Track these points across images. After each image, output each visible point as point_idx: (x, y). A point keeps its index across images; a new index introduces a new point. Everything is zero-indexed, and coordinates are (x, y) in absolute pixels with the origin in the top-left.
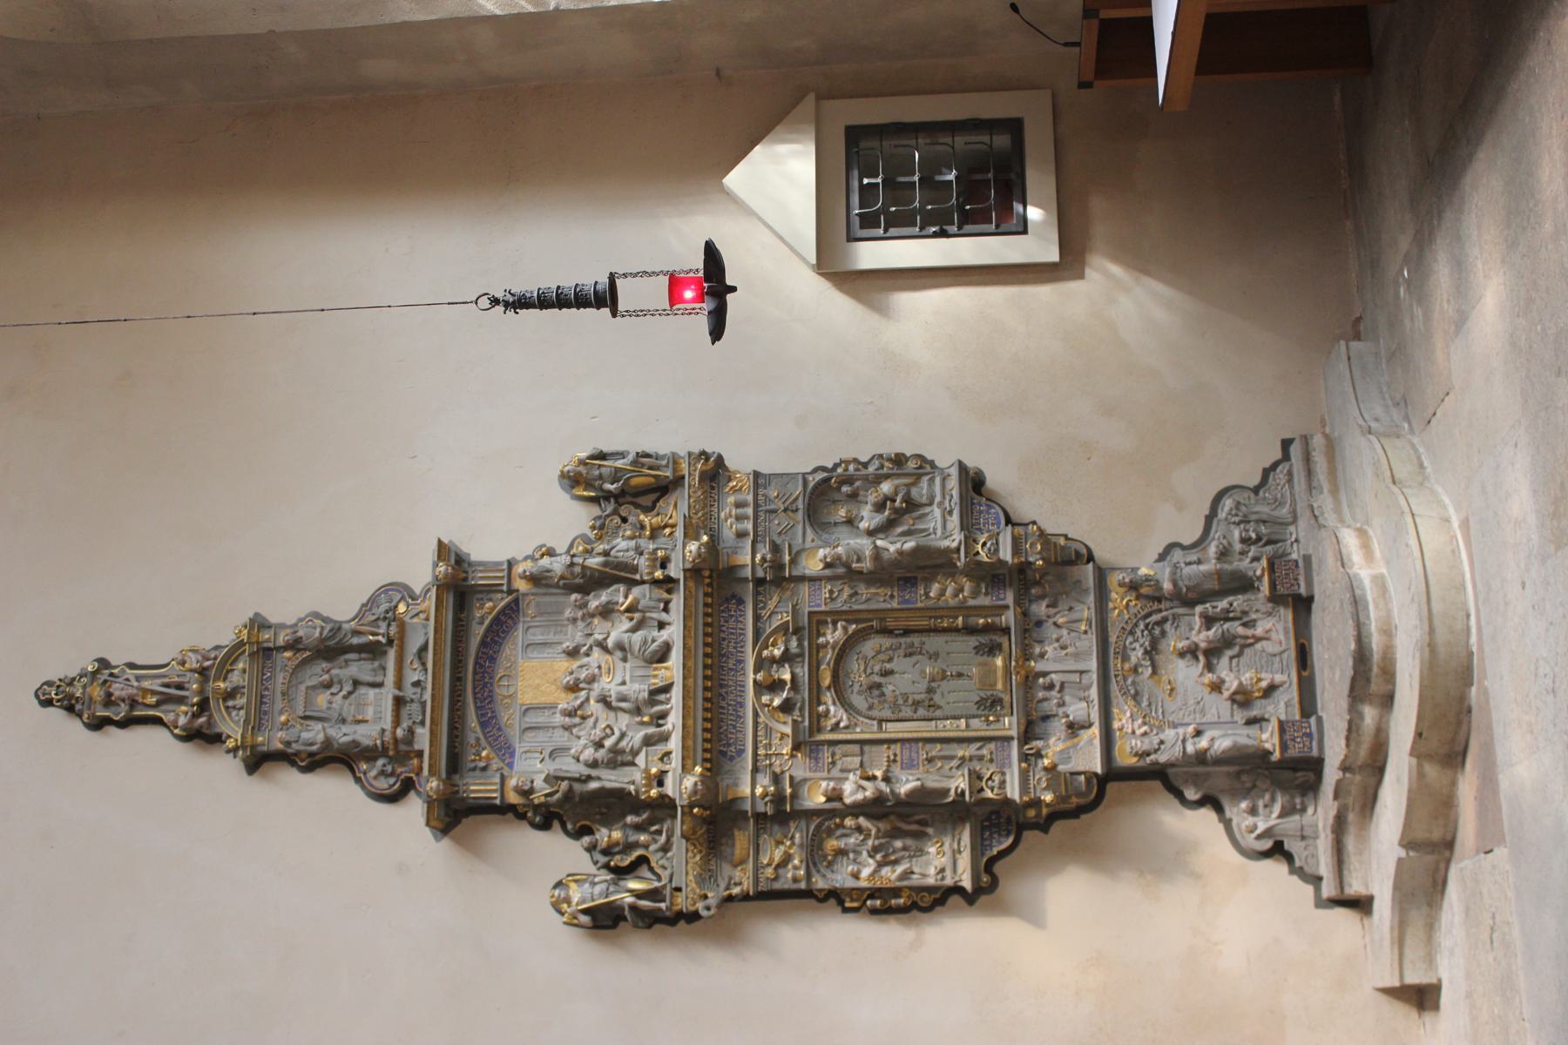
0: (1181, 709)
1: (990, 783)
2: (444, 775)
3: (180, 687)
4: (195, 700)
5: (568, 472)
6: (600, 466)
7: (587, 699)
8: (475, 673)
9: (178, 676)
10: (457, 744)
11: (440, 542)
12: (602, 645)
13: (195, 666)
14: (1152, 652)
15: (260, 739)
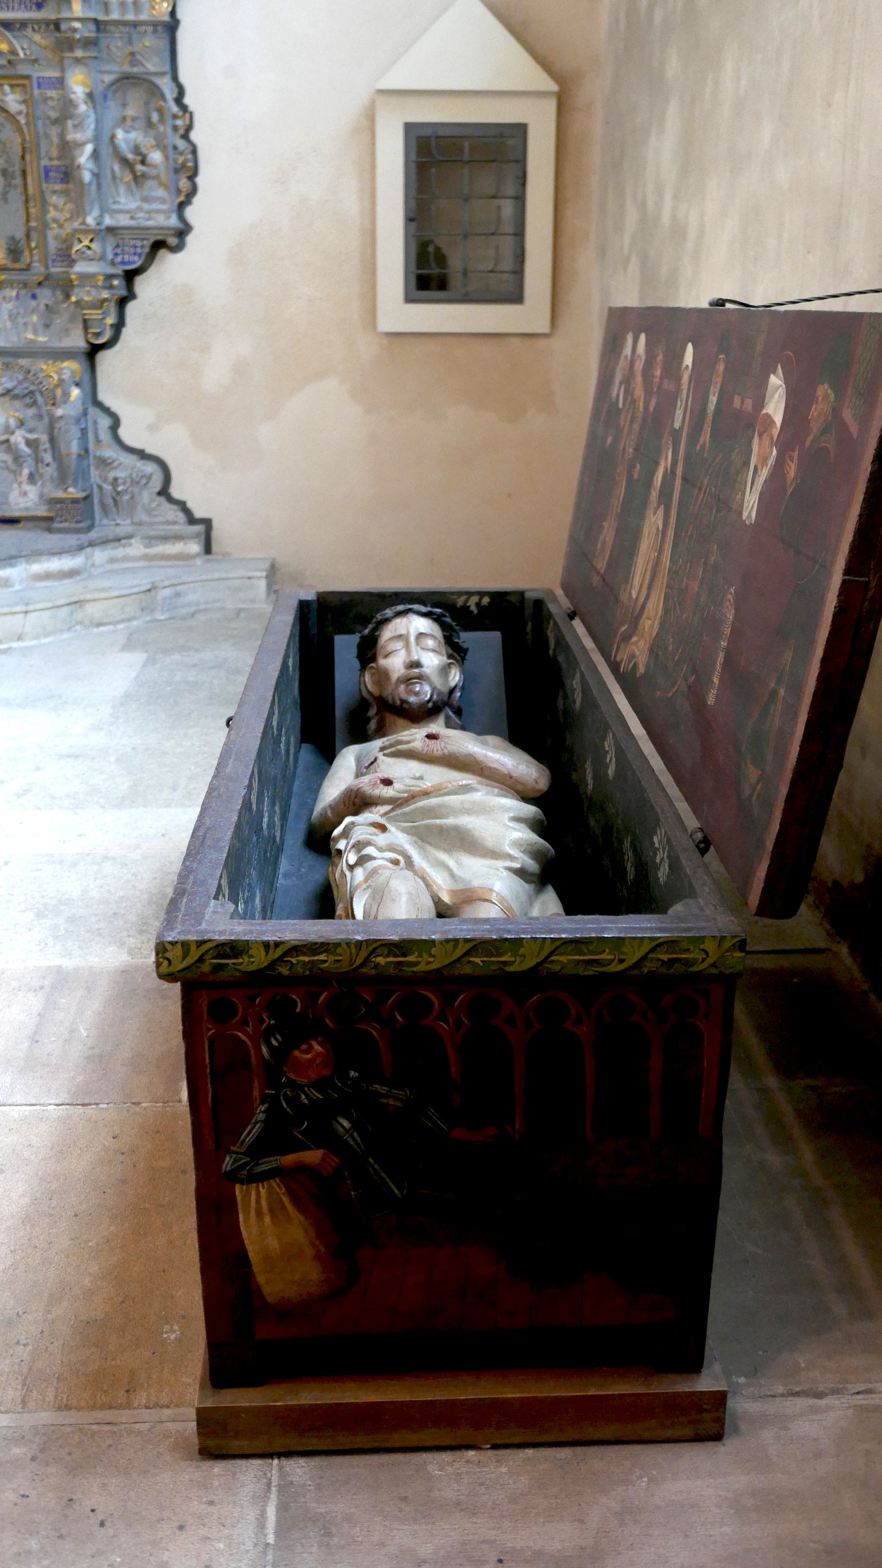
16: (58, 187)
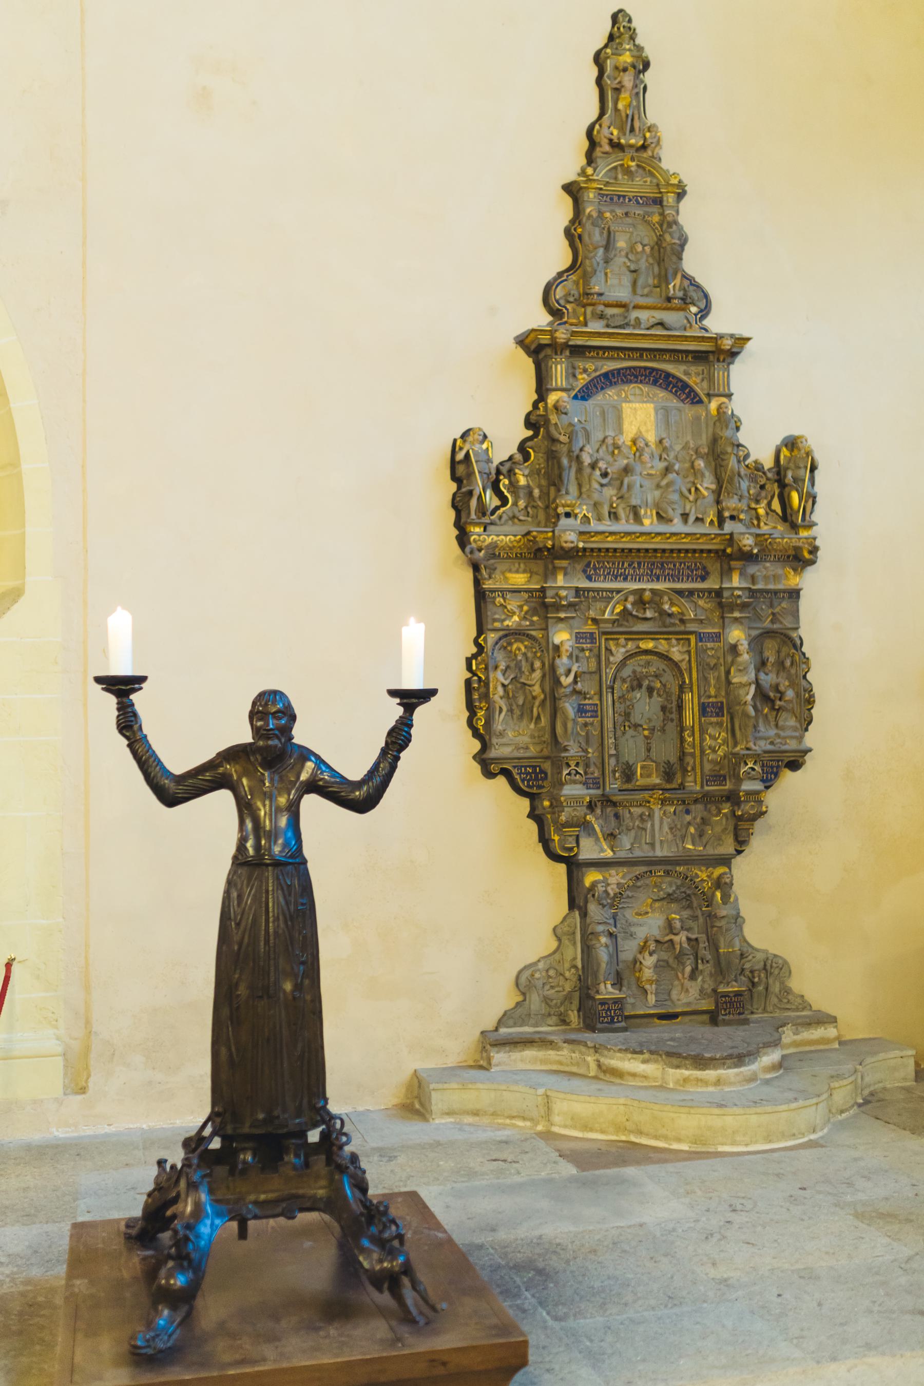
0: (627, 921)
1: (574, 772)
2: (571, 343)
3: (632, 130)
4: (623, 141)
5: (802, 442)
6: (806, 467)
8: (645, 368)
9: (640, 128)
10: (592, 354)
11: (749, 339)
12: (668, 470)
13: (649, 141)
15: (591, 195)
16: (714, 719)
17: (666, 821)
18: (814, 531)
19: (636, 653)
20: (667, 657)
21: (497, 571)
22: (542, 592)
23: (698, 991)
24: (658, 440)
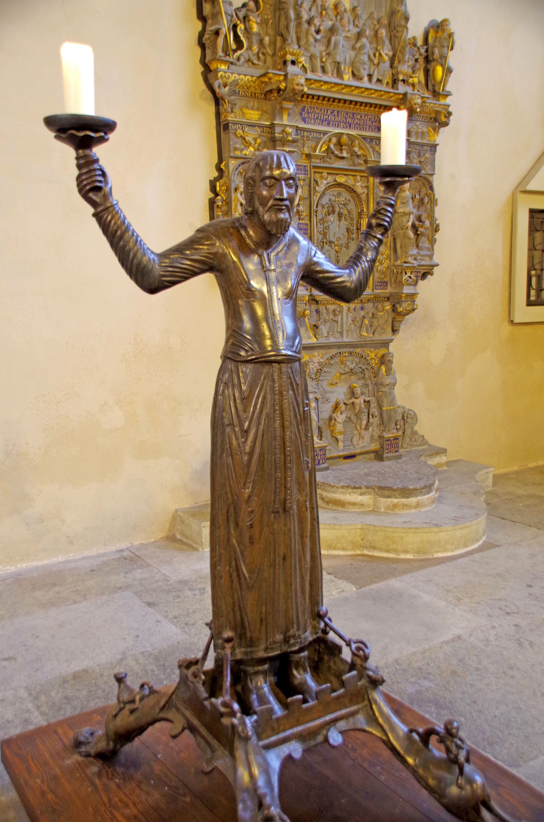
7: (332, 20)
12: (359, 35)
14: (352, 372)
17: (350, 315)
18: (448, 100)
19: (332, 185)
20: (352, 190)
21: (237, 107)
22: (270, 128)
23: (370, 438)
24: (351, 7)
